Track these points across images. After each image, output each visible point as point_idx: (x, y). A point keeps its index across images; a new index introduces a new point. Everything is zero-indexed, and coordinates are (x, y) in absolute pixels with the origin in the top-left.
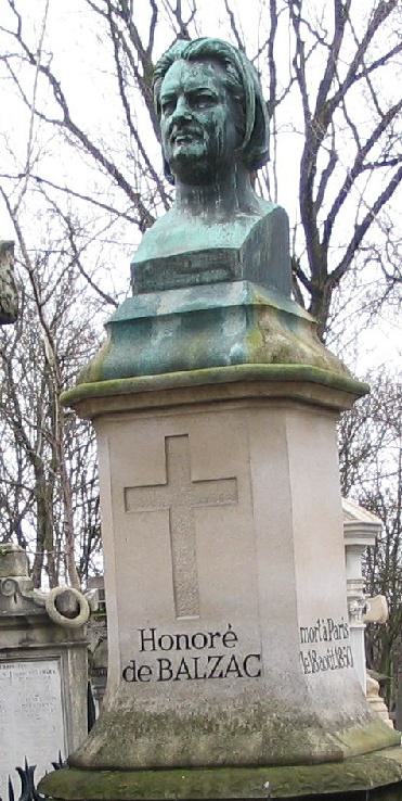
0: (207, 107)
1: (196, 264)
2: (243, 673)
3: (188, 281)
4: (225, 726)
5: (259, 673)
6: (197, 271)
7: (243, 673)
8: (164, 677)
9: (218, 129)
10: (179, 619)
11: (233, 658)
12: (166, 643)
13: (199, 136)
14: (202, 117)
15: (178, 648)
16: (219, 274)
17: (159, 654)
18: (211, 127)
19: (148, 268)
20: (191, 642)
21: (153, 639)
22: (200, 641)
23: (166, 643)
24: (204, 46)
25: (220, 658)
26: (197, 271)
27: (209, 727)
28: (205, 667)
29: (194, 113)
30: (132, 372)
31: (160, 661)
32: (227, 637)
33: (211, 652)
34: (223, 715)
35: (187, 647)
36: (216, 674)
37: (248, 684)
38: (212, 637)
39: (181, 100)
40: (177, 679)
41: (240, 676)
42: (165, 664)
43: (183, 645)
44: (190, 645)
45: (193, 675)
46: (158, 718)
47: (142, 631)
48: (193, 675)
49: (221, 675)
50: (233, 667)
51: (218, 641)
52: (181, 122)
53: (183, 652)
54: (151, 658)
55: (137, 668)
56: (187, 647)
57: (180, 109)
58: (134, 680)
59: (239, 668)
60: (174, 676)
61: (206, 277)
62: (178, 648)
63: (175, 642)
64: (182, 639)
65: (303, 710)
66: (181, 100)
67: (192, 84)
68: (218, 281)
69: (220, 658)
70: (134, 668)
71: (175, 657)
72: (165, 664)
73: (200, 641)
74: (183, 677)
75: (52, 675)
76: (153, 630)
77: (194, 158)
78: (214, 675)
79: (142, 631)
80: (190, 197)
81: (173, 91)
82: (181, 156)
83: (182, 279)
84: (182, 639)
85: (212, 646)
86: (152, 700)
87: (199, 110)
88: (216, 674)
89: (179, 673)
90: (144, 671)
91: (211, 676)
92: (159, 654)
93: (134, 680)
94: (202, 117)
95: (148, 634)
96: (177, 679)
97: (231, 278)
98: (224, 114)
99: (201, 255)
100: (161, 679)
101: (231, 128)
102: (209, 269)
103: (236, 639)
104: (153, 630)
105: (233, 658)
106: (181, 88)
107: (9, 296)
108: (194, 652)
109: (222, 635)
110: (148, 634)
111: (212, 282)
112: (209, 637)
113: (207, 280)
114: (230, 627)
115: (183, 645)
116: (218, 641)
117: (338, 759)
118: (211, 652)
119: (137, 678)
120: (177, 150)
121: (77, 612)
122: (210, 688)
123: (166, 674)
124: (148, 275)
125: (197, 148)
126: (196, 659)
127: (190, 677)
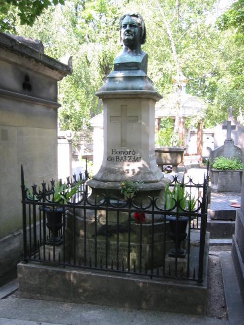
6: (130, 67)
9: (136, 34)
13: (132, 35)
14: (133, 30)
16: (136, 68)
17: (117, 155)
18: (135, 33)
23: (118, 153)
26: (130, 67)
30: (115, 89)
33: (129, 156)
39: (128, 26)
52: (128, 31)
54: (114, 156)
57: (128, 28)
61: (132, 68)
63: (120, 153)
66: (128, 26)
82: (127, 39)
83: (126, 68)
92: (117, 155)
94: (133, 30)
95: (114, 150)
97: (138, 69)
101: (139, 34)
106: (128, 23)
110: (114, 150)
111: (134, 70)
117: (157, 182)
123: (118, 160)
125: (131, 37)
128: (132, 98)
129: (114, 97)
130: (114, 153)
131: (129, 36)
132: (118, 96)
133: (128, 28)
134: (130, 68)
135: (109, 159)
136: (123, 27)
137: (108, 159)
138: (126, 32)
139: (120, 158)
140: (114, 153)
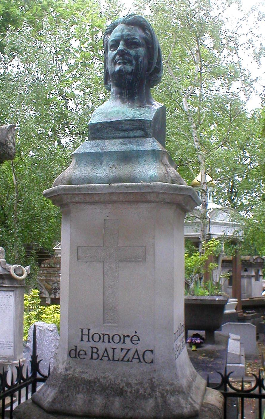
0: (135, 48)
2: (142, 360)
3: (121, 135)
4: (131, 392)
5: (152, 362)
7: (142, 360)
8: (93, 358)
9: (140, 59)
10: (105, 325)
11: (137, 351)
12: (96, 338)
13: (130, 62)
14: (132, 52)
15: (103, 341)
17: (92, 344)
18: (137, 58)
19: (99, 126)
20: (111, 339)
21: (88, 335)
22: (117, 339)
23: (96, 338)
24: (134, 18)
25: (129, 350)
26: (126, 130)
27: (121, 393)
28: (119, 355)
29: (128, 50)
31: (92, 348)
32: (133, 339)
33: (123, 346)
34: (129, 385)
35: (109, 342)
36: (126, 359)
37: (145, 368)
38: (124, 336)
39: (121, 43)
40: (101, 359)
41: (140, 361)
42: (95, 350)
43: (106, 340)
44: (111, 341)
45: (111, 357)
46: (90, 382)
47: (82, 329)
48: (111, 357)
49: (128, 361)
50: (136, 356)
51: (128, 340)
52: (122, 54)
53: (106, 345)
54: (86, 346)
55: (78, 351)
56: (109, 342)
58: (76, 357)
59: (140, 357)
60: (100, 358)
61: (131, 134)
62: (103, 341)
63: (102, 338)
64: (106, 337)
65: (175, 383)
66: (121, 43)
67: (128, 35)
68: (138, 137)
69: (129, 350)
70: (76, 350)
71: (101, 346)
72: (95, 350)
73: (117, 339)
74: (105, 359)
75: (11, 297)
76: (89, 330)
77: (128, 73)
78: (124, 360)
79: (82, 329)
80: (121, 94)
81: (118, 38)
82: (120, 71)
84: (106, 337)
85: (124, 342)
86: (86, 370)
87: (131, 48)
88: (126, 359)
89: (103, 356)
90: (82, 353)
91: (122, 360)
92: (92, 344)
93: (76, 357)
94: (132, 52)
95: (85, 332)
96: (101, 359)
97: (146, 135)
98: (143, 52)
99: (129, 122)
100: (92, 358)
101: (146, 61)
102: (133, 130)
103: (139, 340)
104: (89, 330)
105: (137, 351)
106: (122, 36)
107: (12, 148)
108: (112, 345)
109: (131, 337)
110: (85, 332)
111: (135, 137)
112: (122, 337)
113: (132, 135)
114: (136, 332)
115: (106, 340)
116: (128, 340)
118: (123, 346)
119: (77, 357)
120: (118, 67)
121: (21, 275)
122: (121, 368)
123: (95, 356)
124: (98, 130)
125: (129, 68)
126: (114, 349)
127: (109, 359)
128: (130, 202)
129: (88, 199)
130: (85, 338)
131: (124, 63)
132: (97, 198)
133: (121, 47)
134: (126, 134)
135: (73, 355)
136: (112, 46)
137: (70, 354)
138: (118, 57)
139: (101, 353)
140: (85, 338)
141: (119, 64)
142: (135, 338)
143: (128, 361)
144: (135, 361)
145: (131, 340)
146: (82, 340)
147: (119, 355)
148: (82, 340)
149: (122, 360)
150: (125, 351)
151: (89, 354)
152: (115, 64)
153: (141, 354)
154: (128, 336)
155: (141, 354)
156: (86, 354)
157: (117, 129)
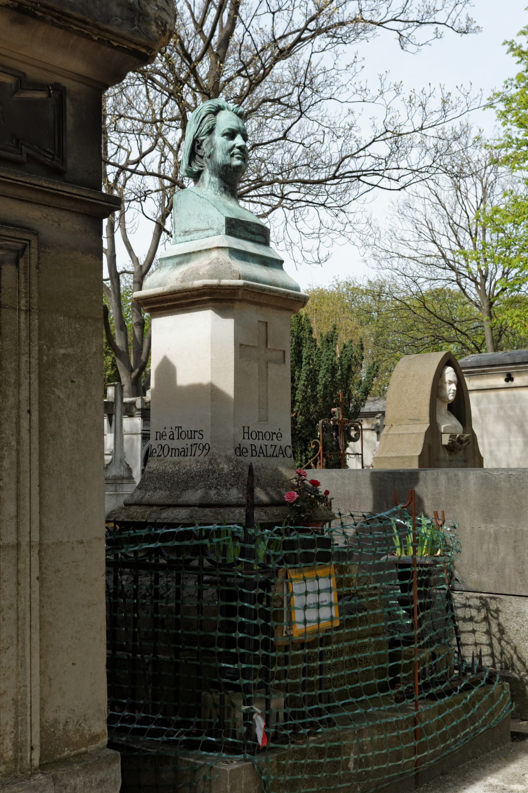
1: (254, 230)
3: (249, 237)
12: (254, 436)
17: (251, 441)
19: (234, 222)
23: (254, 436)
26: (253, 233)
28: (270, 451)
31: (251, 445)
42: (253, 448)
45: (265, 454)
54: (247, 443)
58: (240, 455)
64: (261, 434)
70: (240, 448)
72: (253, 448)
74: (261, 455)
80: (225, 188)
88: (275, 455)
95: (246, 431)
100: (252, 456)
110: (246, 431)
118: (271, 442)
139: (258, 449)
140: (246, 436)
141: (238, 158)
142: (279, 435)
143: (276, 456)
144: (281, 456)
145: (277, 437)
146: (244, 438)
147: (270, 451)
148: (244, 438)
149: (273, 456)
150: (273, 447)
151: (250, 451)
152: (232, 155)
153: (283, 449)
154: (275, 433)
155: (283, 449)
156: (247, 452)
157: (247, 230)
